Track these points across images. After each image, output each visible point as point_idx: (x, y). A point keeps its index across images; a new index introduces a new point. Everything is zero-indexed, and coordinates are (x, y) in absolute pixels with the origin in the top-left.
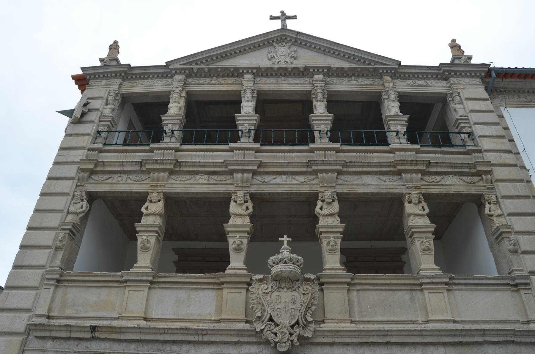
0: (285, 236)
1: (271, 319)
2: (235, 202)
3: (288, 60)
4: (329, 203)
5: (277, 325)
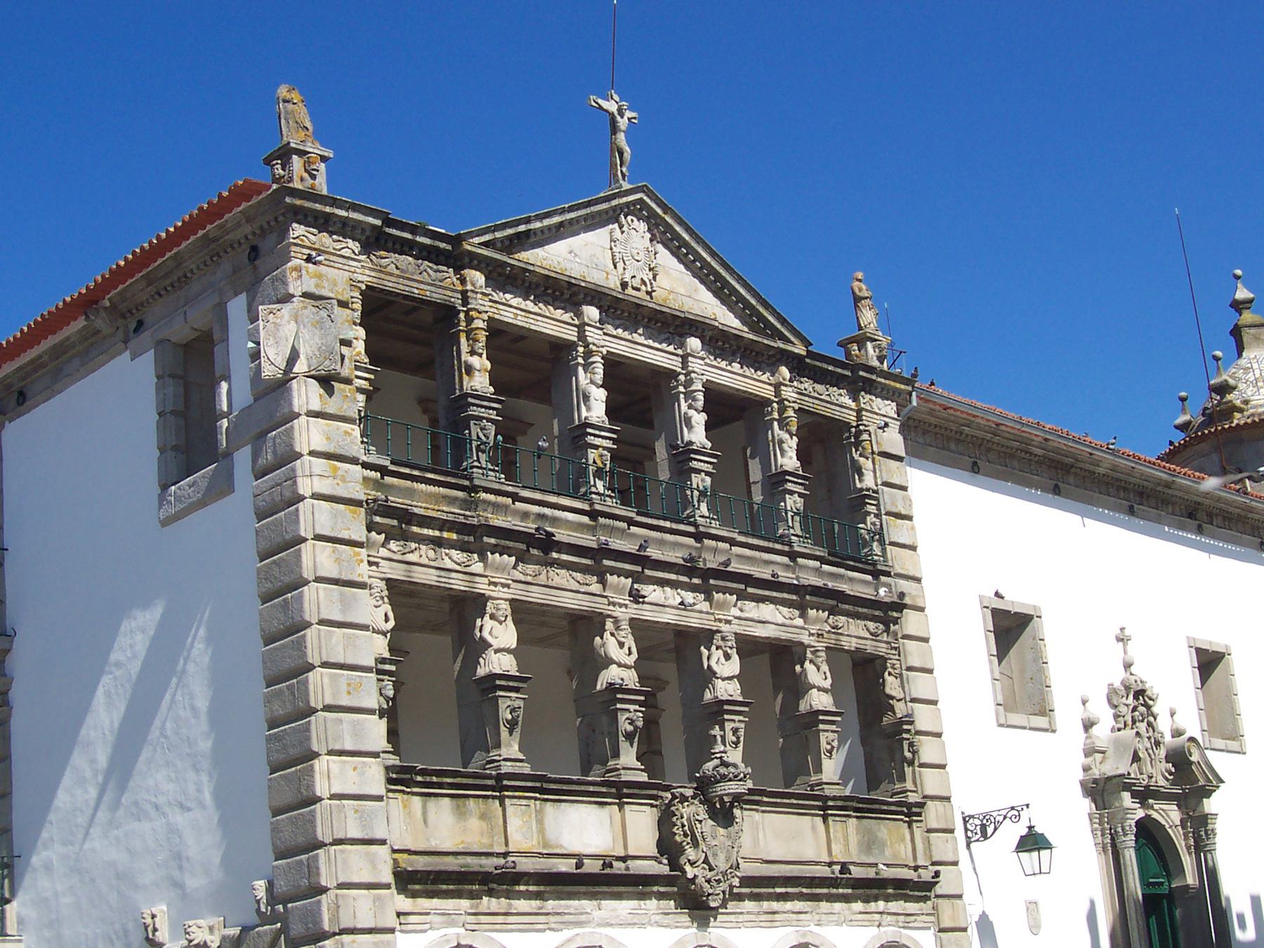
1: (706, 861)
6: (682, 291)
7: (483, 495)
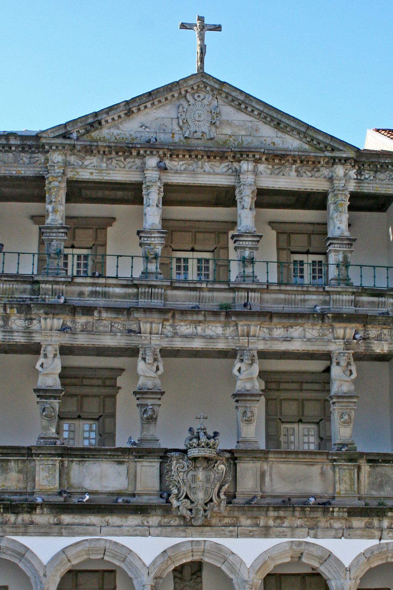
1: (187, 497)
2: (144, 359)
5: (192, 502)
6: (243, 133)
7: (43, 286)
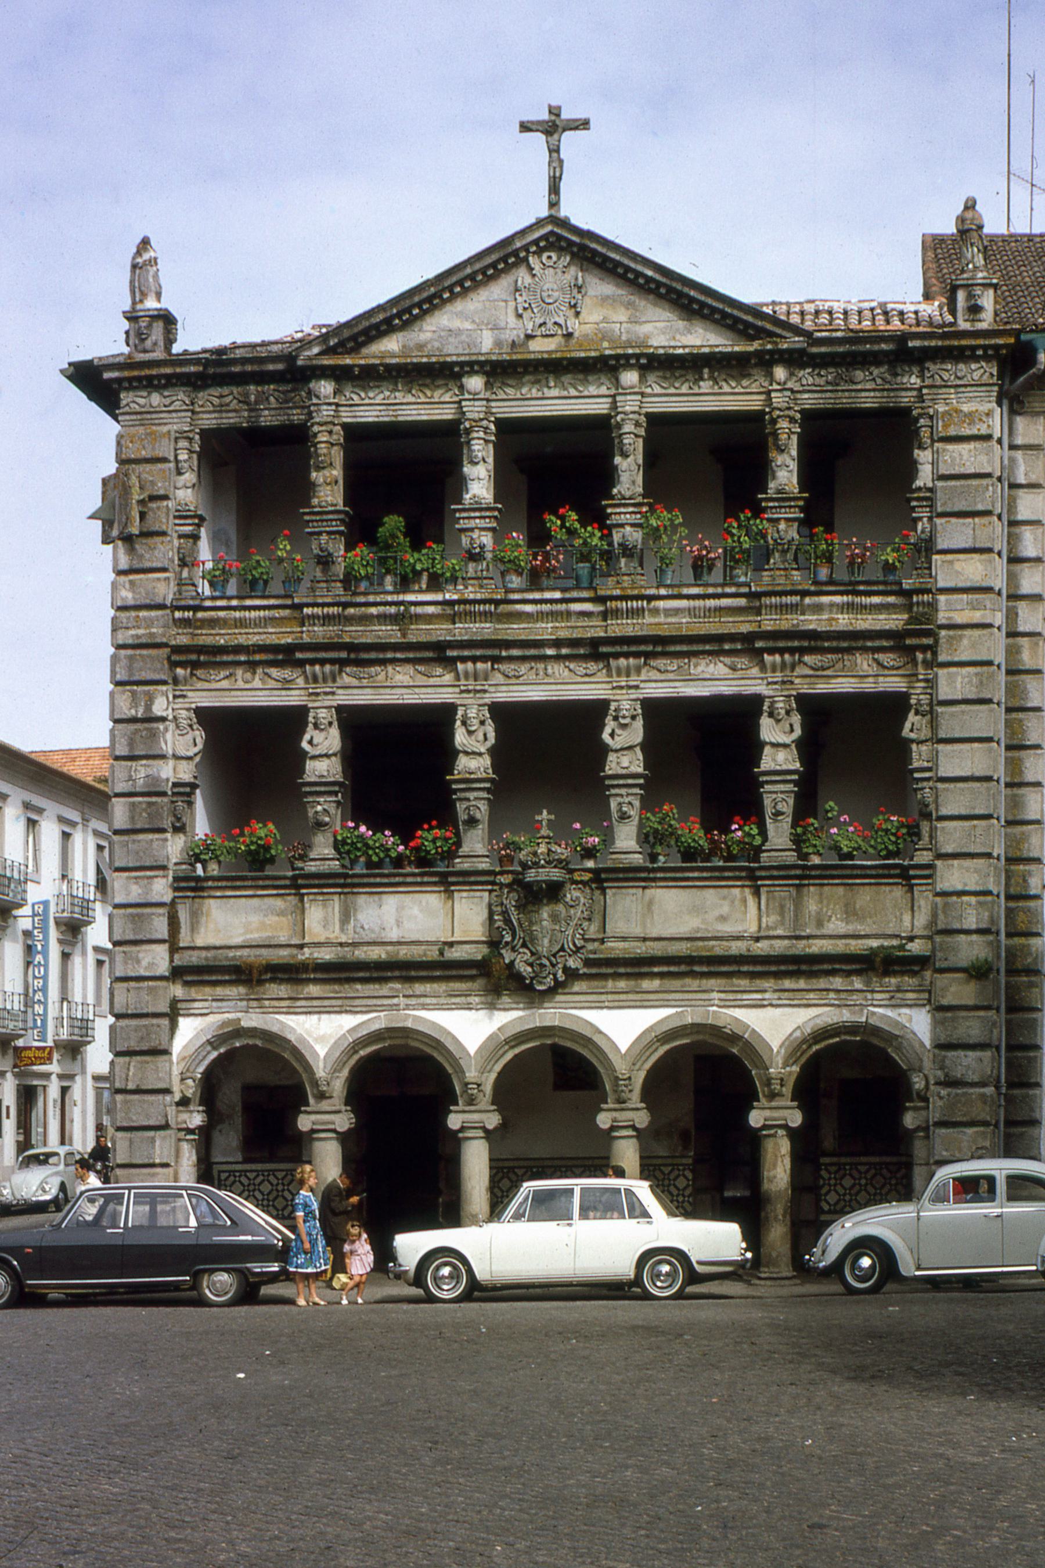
0: (545, 812)
3: (561, 321)
4: (624, 726)
